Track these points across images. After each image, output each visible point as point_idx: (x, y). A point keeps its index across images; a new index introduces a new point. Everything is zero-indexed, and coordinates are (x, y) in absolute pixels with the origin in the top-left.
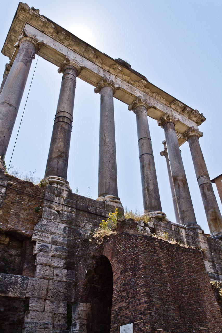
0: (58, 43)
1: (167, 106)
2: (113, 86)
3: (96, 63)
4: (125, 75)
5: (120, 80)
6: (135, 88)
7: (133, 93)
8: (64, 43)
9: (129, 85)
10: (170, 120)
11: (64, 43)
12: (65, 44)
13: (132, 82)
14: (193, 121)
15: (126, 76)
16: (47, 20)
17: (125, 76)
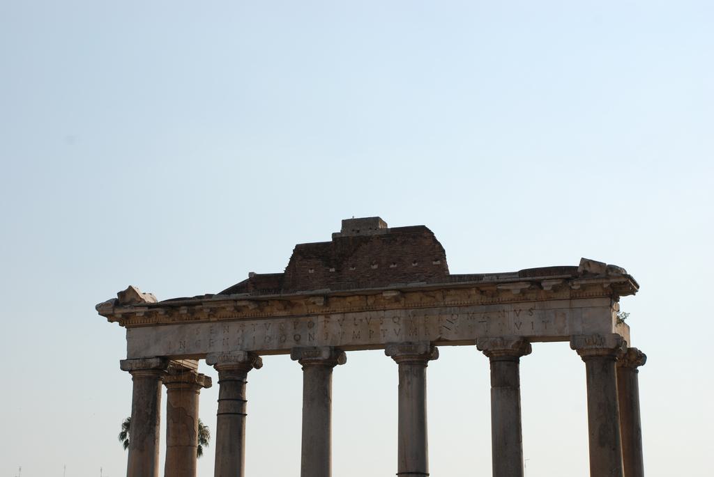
0: (190, 325)
1: (487, 304)
2: (318, 361)
3: (275, 314)
4: (344, 297)
5: (339, 317)
6: (382, 313)
7: (374, 341)
8: (199, 319)
9: (364, 314)
10: (495, 355)
11: (199, 319)
12: (202, 319)
13: (371, 301)
14: (591, 297)
15: (349, 296)
16: (146, 309)
17: (349, 299)
